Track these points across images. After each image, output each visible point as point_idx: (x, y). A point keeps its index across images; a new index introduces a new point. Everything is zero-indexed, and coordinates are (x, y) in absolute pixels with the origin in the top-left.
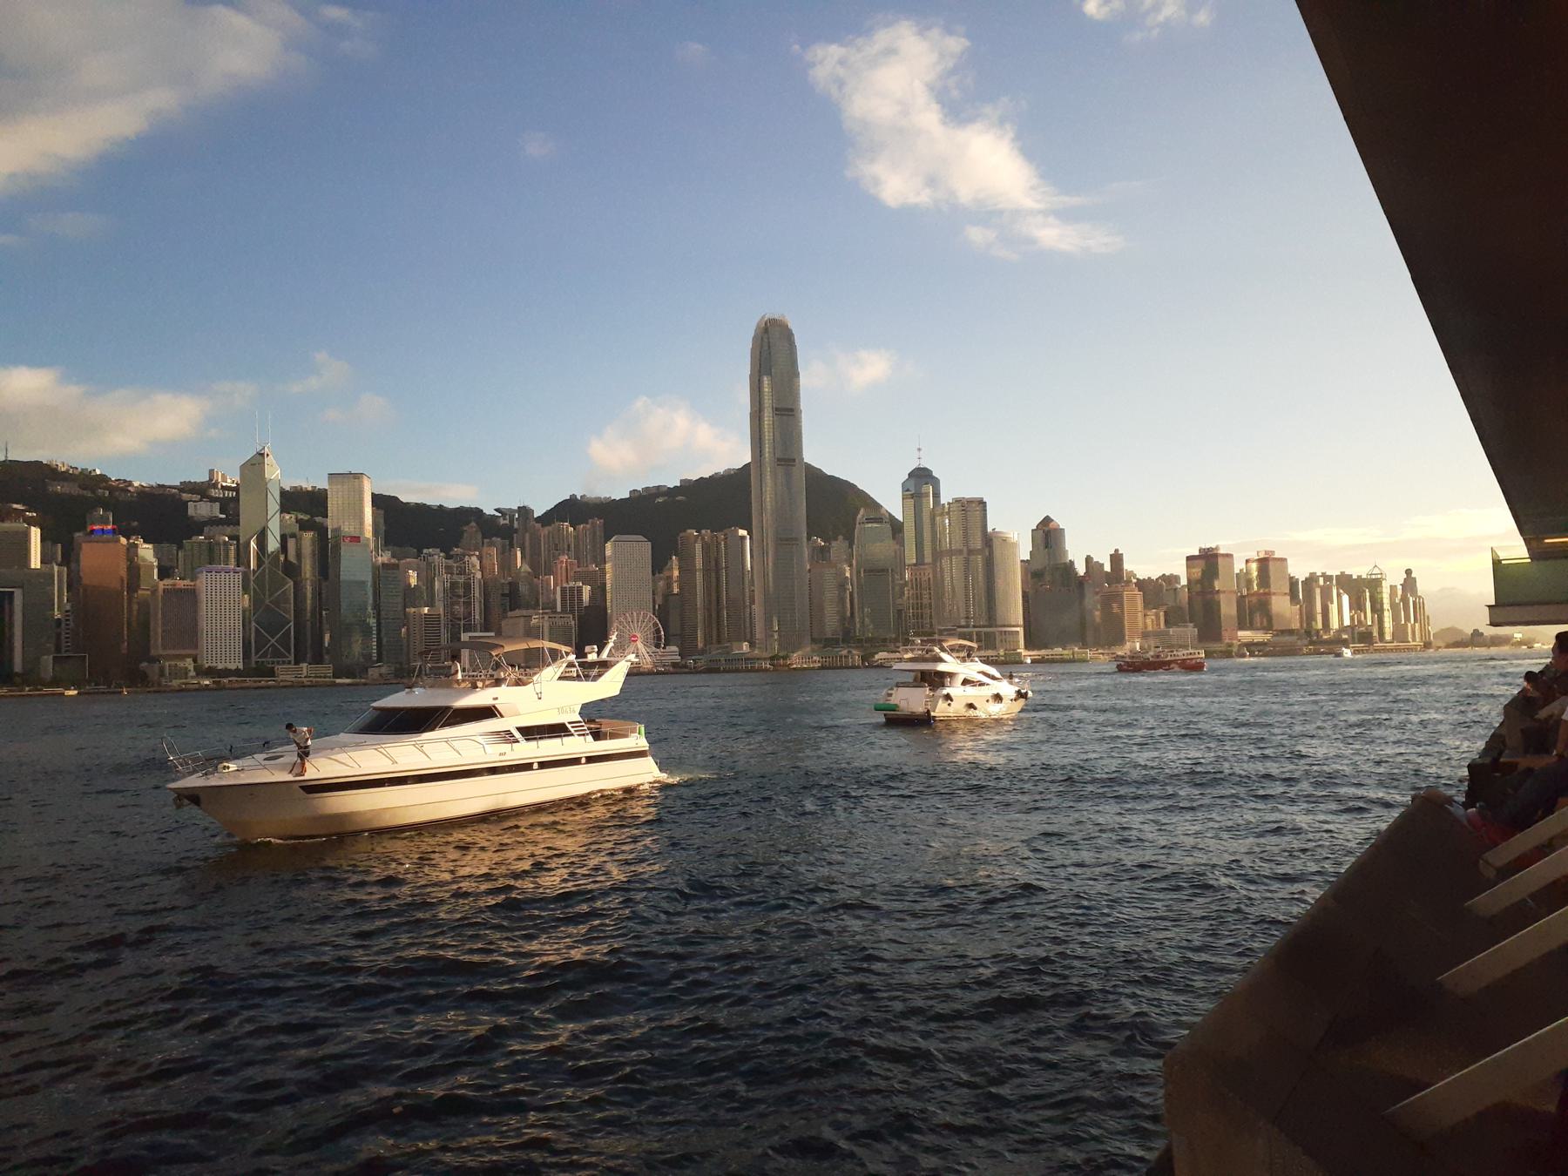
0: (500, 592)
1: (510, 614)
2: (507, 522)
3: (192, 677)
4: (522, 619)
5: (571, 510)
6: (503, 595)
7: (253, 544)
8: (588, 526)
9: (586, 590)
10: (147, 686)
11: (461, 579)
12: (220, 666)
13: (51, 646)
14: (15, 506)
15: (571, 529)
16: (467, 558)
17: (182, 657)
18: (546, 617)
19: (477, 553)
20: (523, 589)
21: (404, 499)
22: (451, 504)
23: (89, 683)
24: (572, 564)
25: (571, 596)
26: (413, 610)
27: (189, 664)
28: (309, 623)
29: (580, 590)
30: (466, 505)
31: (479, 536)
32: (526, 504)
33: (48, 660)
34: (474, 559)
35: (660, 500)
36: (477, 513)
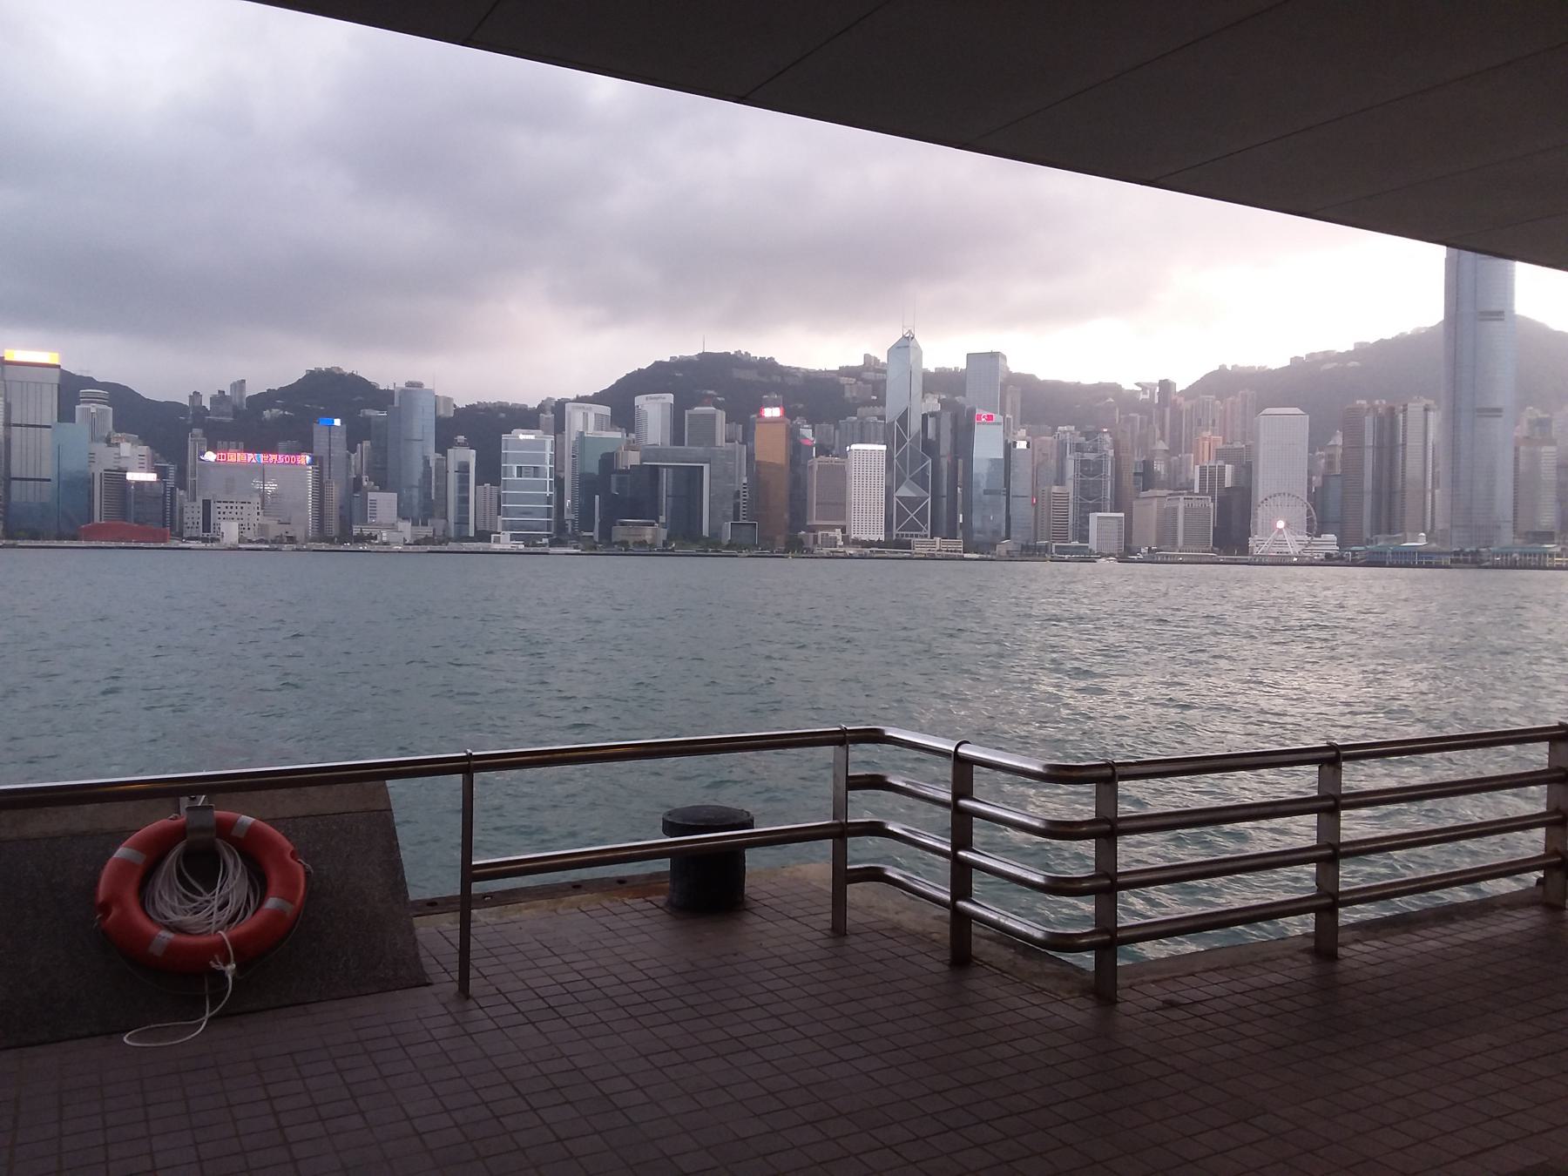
0: (1134, 471)
1: (1143, 494)
3: (840, 546)
6: (1136, 474)
9: (1229, 468)
10: (802, 553)
12: (864, 537)
13: (730, 513)
14: (710, 392)
20: (1159, 467)
23: (756, 547)
24: (1215, 441)
27: (838, 533)
28: (945, 499)
29: (1222, 470)
33: (727, 526)
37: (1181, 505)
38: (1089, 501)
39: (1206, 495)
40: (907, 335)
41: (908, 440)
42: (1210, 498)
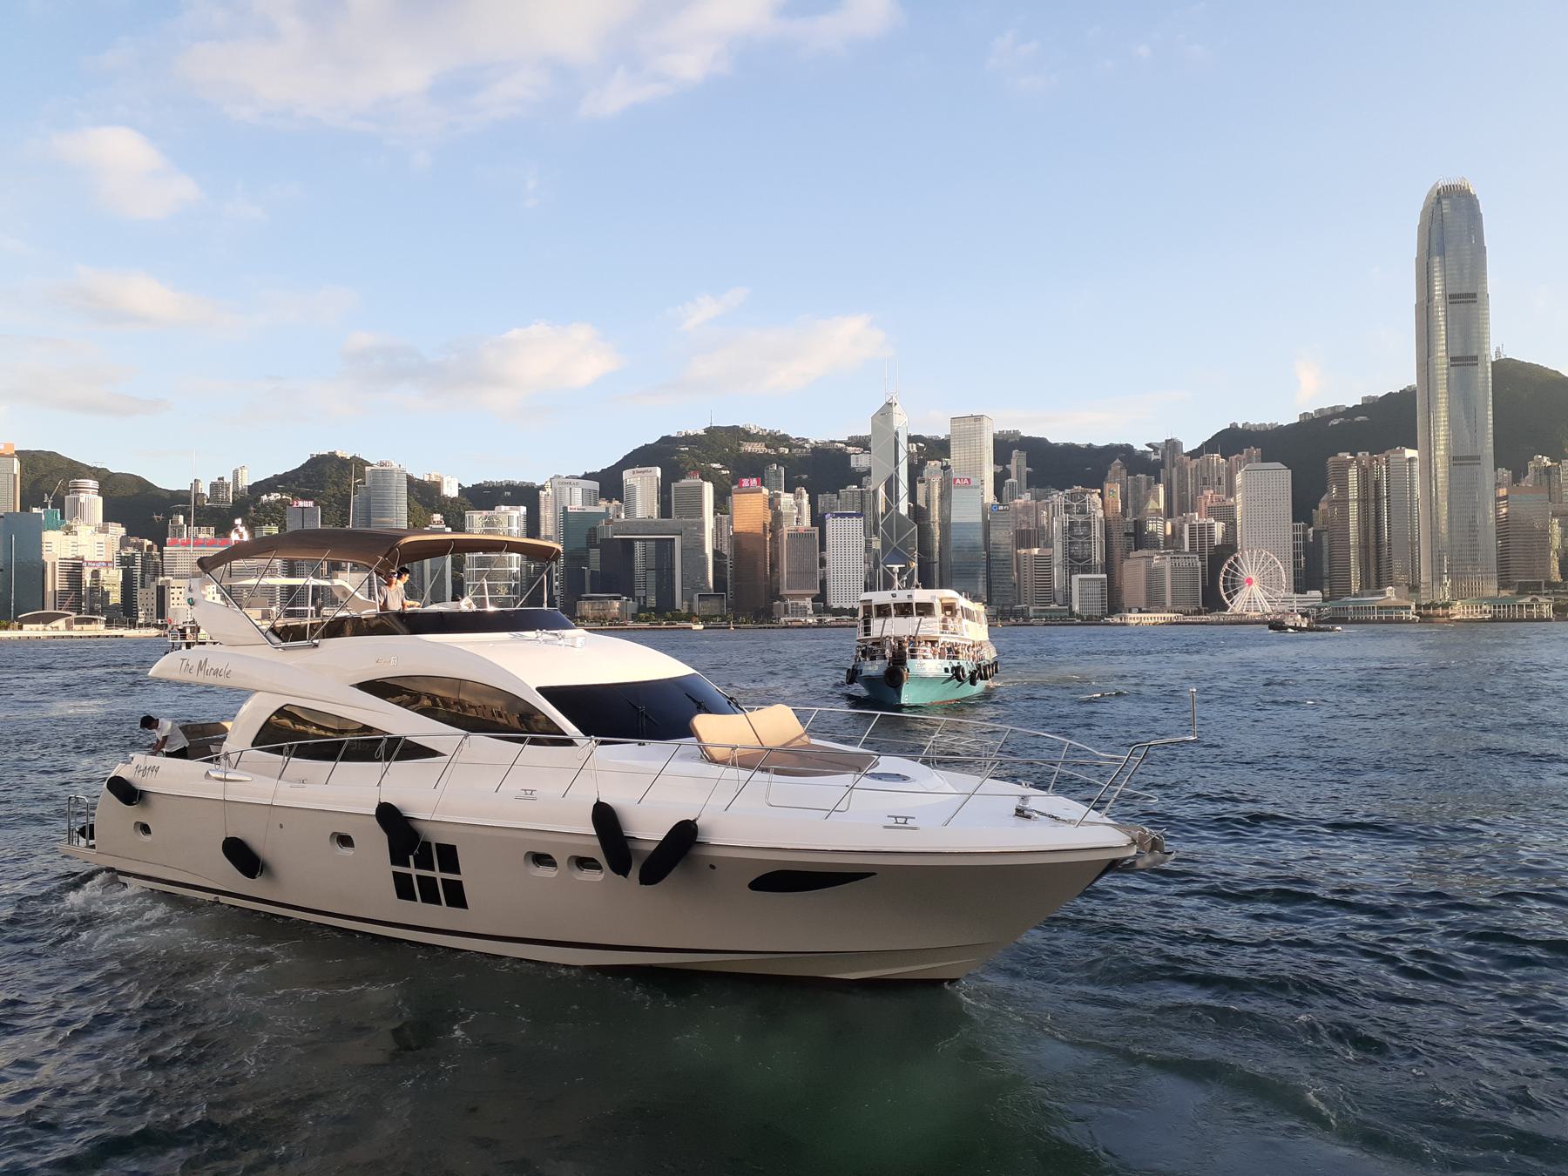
0: (1126, 531)
1: (1132, 554)
2: (1159, 457)
4: (1143, 562)
5: (1231, 442)
6: (1127, 534)
7: (882, 491)
8: (1244, 456)
9: (1219, 528)
11: (1080, 519)
15: (1222, 460)
16: (1087, 496)
17: (802, 597)
18: (1168, 557)
19: (1099, 491)
21: (1052, 440)
22: (1100, 442)
25: (1202, 532)
26: (1023, 551)
29: (1210, 527)
30: (1116, 442)
31: (1124, 472)
32: (1174, 436)
34: (1096, 497)
35: (1335, 422)
36: (1125, 452)
37: (1167, 564)
38: (1077, 563)
39: (1193, 554)
40: (891, 402)
41: (894, 506)
42: (1197, 556)
